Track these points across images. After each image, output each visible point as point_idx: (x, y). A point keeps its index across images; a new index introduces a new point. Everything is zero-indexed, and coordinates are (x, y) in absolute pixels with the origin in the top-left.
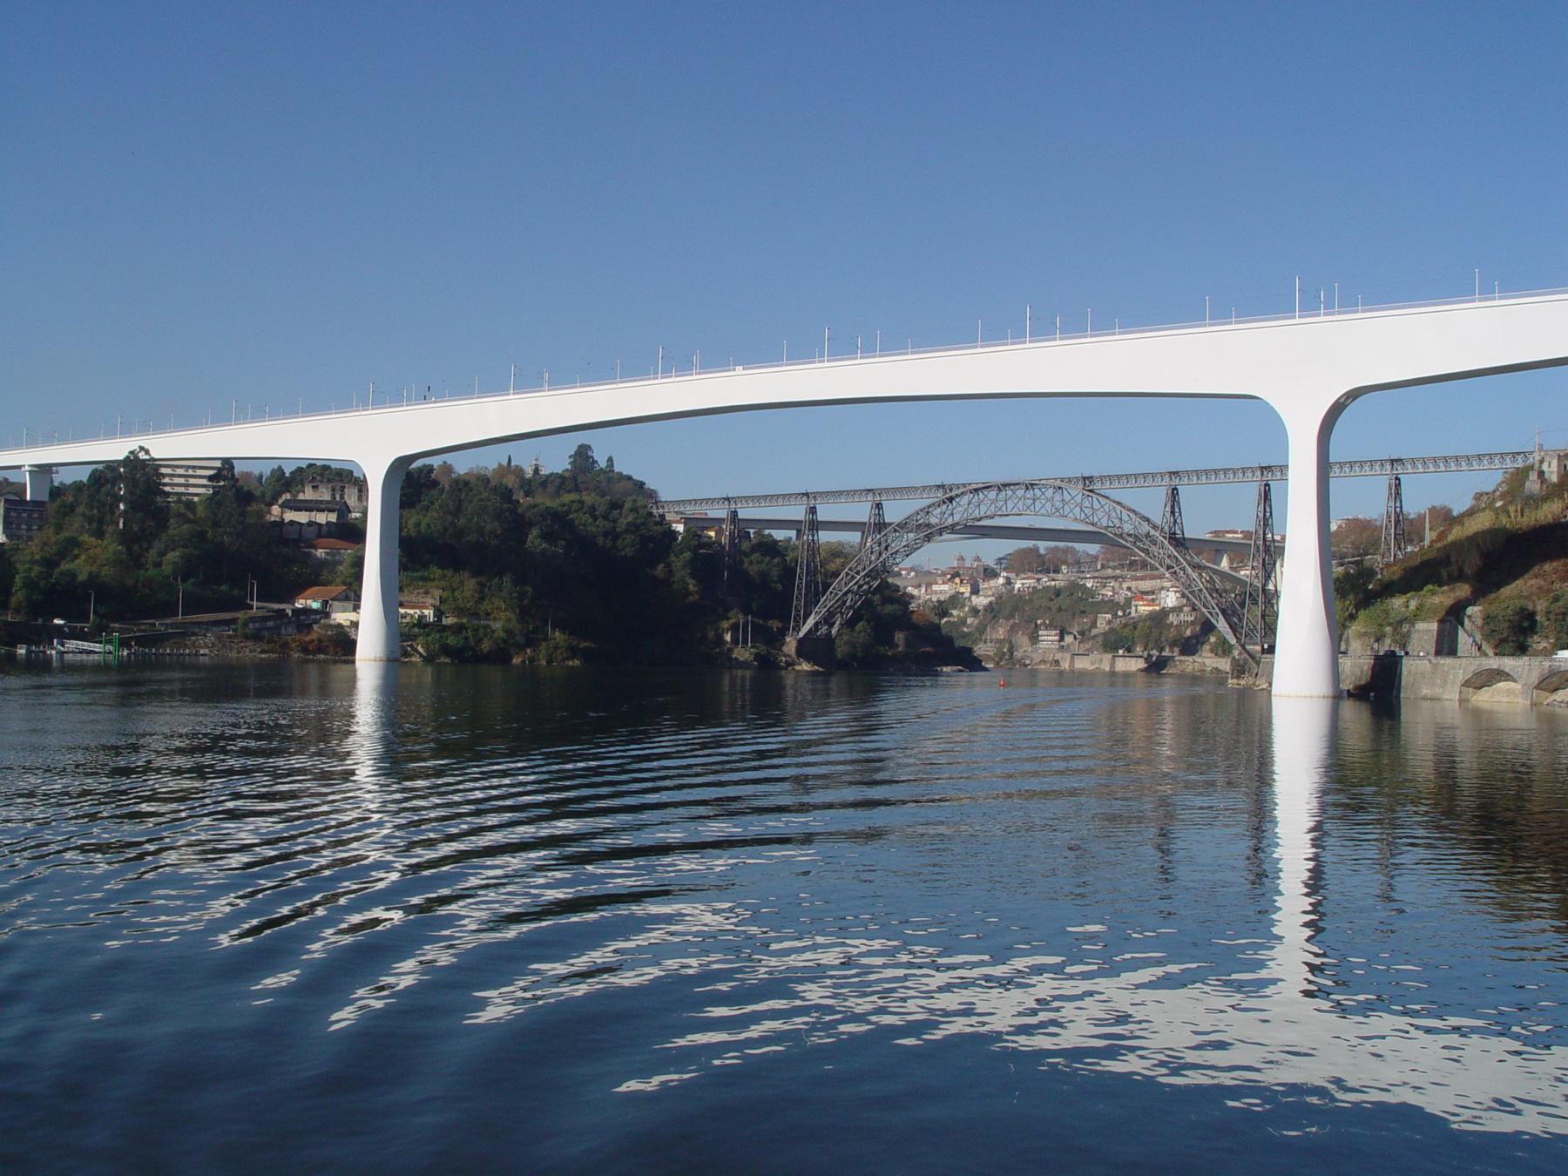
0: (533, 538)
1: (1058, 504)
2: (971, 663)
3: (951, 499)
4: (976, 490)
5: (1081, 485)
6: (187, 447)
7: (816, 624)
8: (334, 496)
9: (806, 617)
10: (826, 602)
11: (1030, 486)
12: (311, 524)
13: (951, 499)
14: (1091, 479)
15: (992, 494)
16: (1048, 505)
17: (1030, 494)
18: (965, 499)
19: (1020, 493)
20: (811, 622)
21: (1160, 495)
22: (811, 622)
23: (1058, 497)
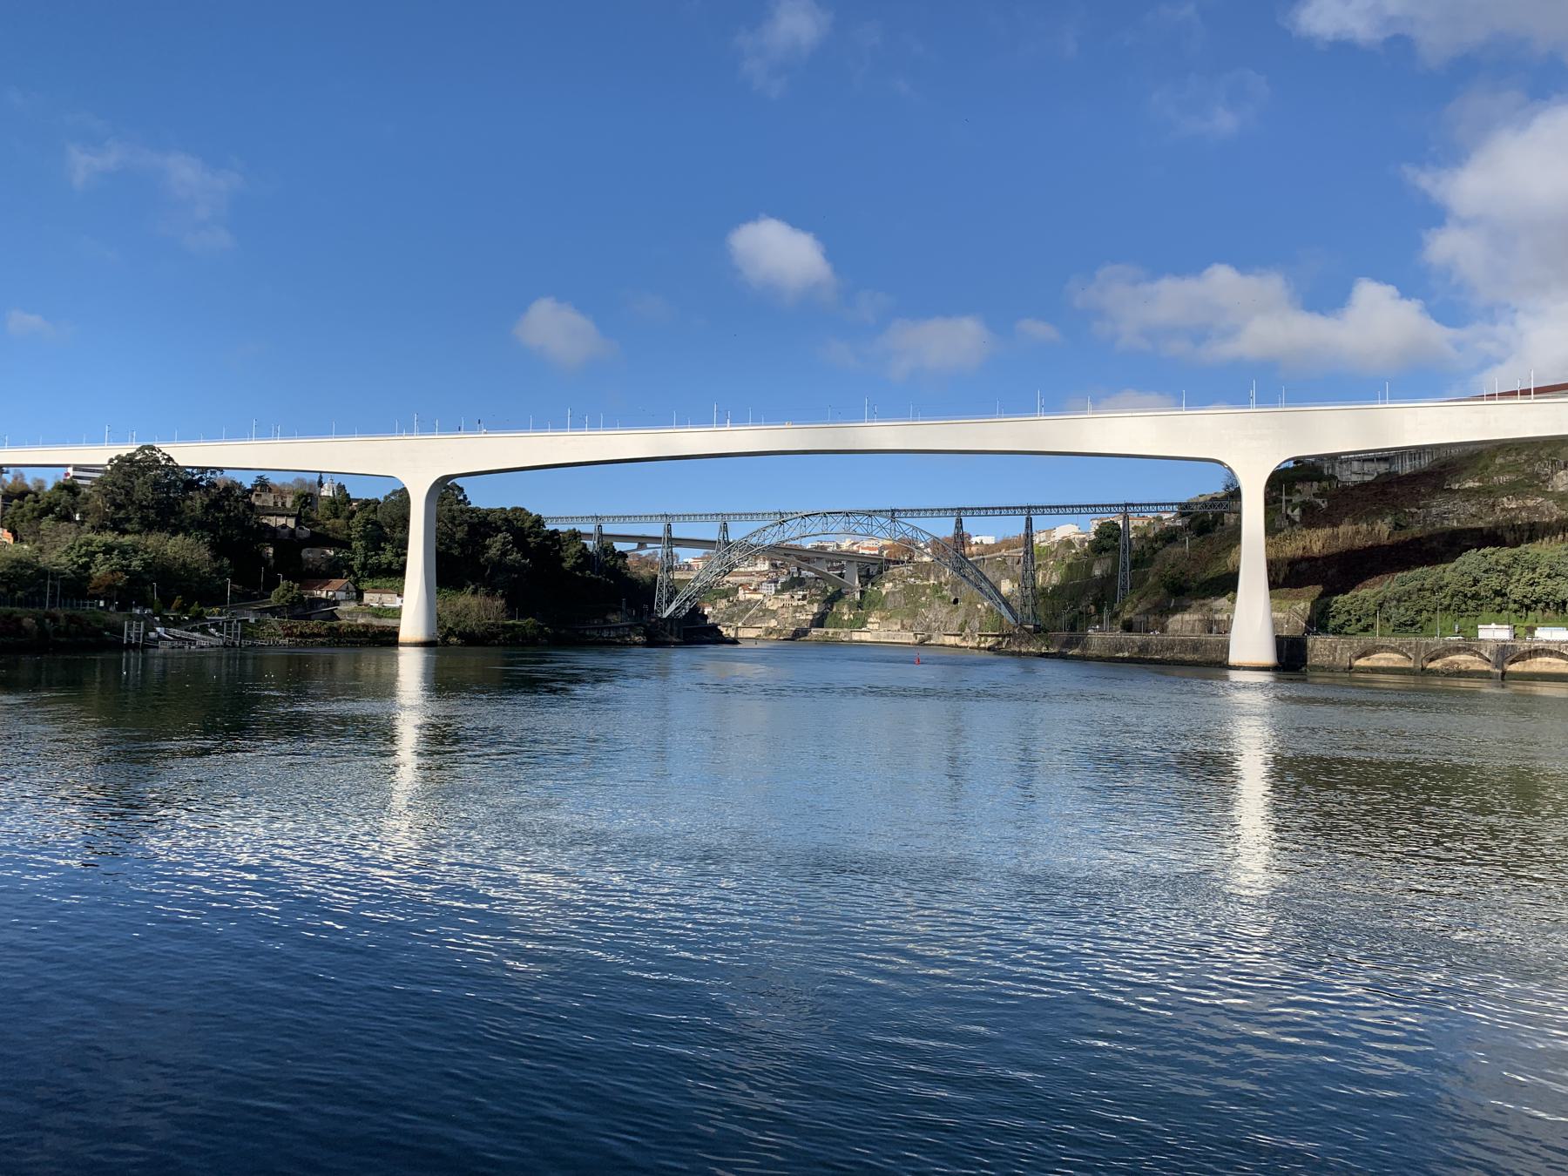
6: (188, 454)
9: (669, 602)
12: (284, 526)
20: (673, 606)
22: (673, 606)
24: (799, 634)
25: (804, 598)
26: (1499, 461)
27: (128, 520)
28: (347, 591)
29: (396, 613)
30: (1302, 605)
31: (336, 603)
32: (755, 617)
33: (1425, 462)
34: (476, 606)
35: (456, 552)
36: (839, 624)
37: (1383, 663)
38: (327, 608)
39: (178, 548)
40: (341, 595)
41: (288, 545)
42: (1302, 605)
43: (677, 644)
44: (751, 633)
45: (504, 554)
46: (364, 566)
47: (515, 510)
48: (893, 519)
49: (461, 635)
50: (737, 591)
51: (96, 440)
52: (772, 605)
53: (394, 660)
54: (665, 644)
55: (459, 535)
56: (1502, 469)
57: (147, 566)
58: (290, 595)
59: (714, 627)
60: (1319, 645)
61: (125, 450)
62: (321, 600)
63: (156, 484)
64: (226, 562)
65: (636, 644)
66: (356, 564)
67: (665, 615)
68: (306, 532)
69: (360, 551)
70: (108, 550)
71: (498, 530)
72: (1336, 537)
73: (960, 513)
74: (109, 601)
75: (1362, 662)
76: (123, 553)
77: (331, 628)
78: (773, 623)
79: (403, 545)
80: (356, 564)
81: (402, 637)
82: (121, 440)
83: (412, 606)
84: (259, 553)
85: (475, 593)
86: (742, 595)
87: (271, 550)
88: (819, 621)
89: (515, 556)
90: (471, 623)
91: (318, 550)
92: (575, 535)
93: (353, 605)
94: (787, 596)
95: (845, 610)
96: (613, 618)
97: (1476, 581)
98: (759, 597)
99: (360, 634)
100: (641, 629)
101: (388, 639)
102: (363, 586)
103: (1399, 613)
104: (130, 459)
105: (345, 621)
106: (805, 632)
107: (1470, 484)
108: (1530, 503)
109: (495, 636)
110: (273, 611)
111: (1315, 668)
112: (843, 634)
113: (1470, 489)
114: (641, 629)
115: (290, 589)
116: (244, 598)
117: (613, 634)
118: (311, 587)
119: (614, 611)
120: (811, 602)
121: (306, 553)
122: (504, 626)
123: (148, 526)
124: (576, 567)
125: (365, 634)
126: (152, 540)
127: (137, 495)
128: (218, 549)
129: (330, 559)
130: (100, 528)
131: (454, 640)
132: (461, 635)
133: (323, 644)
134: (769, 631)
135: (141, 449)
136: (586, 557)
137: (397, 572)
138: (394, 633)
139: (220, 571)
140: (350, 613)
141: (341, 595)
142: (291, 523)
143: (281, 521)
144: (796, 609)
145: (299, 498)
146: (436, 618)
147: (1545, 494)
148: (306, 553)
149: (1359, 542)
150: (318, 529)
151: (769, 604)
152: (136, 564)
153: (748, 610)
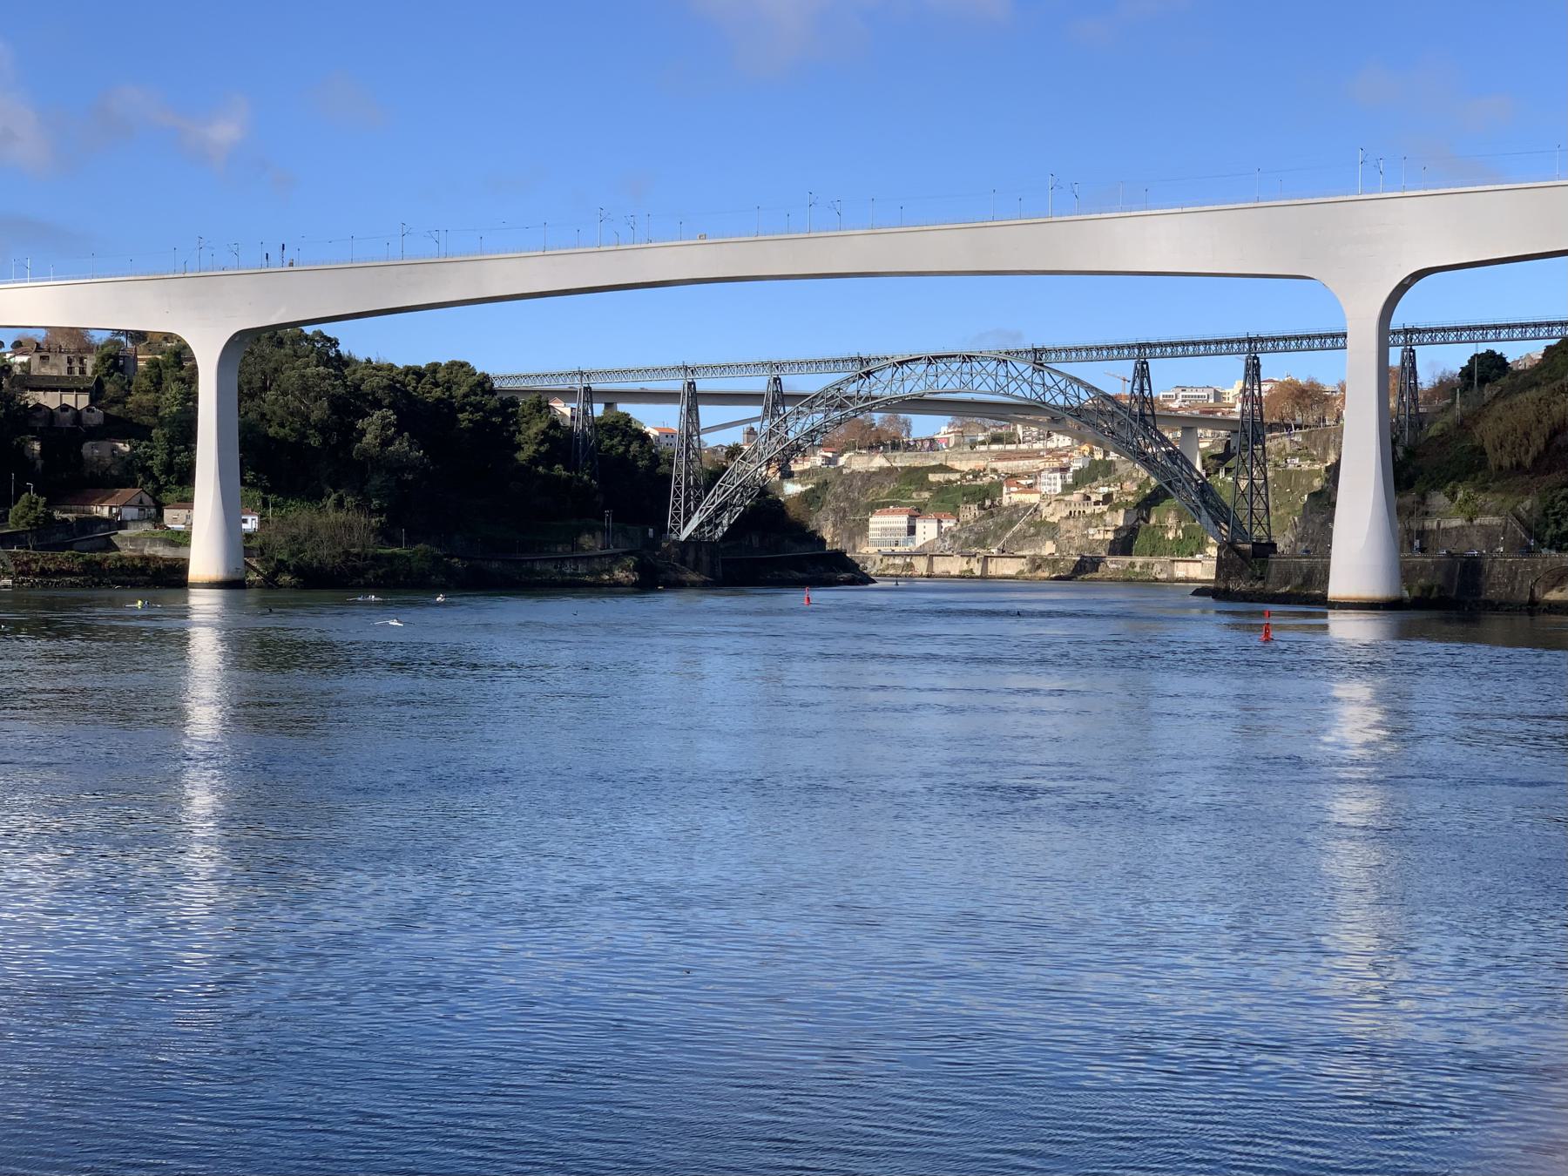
0: (372, 427)
1: (1002, 381)
2: (839, 570)
3: (868, 374)
4: (901, 363)
5: (1030, 357)
7: (701, 525)
8: (70, 370)
9: (688, 516)
10: (714, 499)
13: (868, 374)
14: (1044, 351)
15: (920, 368)
16: (956, 380)
17: (966, 367)
18: (889, 371)
19: (954, 366)
21: (1128, 368)
23: (1002, 371)
24: (1086, 566)
25: (1107, 498)
28: (141, 505)
29: (182, 539)
30: (1528, 503)
31: (123, 525)
32: (1022, 538)
35: (315, 441)
36: (1157, 548)
38: (101, 533)
40: (130, 513)
41: (64, 434)
42: (1528, 503)
44: (1008, 567)
45: (387, 442)
46: (168, 468)
47: (453, 364)
49: (299, 571)
50: (998, 486)
52: (1053, 513)
53: (184, 613)
54: (677, 585)
55: (314, 417)
58: (32, 515)
59: (840, 555)
60: (1497, 568)
62: (101, 520)
65: (618, 584)
66: (155, 464)
67: (684, 536)
68: (97, 417)
69: (163, 443)
71: (377, 404)
73: (1142, 353)
75: (1554, 596)
77: (88, 563)
78: (1049, 548)
83: (205, 532)
84: (21, 448)
85: (340, 504)
86: (1011, 497)
87: (37, 447)
88: (1124, 544)
89: (401, 446)
90: (323, 554)
91: (106, 445)
92: (541, 403)
93: (148, 526)
94: (1076, 496)
95: (1171, 521)
96: (586, 541)
98: (1033, 498)
99: (135, 571)
100: (630, 562)
101: (173, 577)
102: (166, 497)
105: (127, 550)
111: (1495, 607)
114: (630, 562)
115: (32, 506)
117: (582, 568)
118: (89, 501)
119: (591, 531)
120: (1114, 508)
121: (90, 450)
122: (377, 558)
124: (548, 459)
125: (143, 571)
129: (122, 457)
131: (285, 578)
132: (299, 571)
133: (73, 585)
134: (1036, 563)
136: (560, 441)
137: (185, 476)
140: (132, 540)
141: (130, 513)
142: (83, 401)
143: (69, 399)
145: (103, 360)
146: (244, 547)
148: (92, 450)
150: (114, 410)
151: (1046, 511)
153: (1011, 523)
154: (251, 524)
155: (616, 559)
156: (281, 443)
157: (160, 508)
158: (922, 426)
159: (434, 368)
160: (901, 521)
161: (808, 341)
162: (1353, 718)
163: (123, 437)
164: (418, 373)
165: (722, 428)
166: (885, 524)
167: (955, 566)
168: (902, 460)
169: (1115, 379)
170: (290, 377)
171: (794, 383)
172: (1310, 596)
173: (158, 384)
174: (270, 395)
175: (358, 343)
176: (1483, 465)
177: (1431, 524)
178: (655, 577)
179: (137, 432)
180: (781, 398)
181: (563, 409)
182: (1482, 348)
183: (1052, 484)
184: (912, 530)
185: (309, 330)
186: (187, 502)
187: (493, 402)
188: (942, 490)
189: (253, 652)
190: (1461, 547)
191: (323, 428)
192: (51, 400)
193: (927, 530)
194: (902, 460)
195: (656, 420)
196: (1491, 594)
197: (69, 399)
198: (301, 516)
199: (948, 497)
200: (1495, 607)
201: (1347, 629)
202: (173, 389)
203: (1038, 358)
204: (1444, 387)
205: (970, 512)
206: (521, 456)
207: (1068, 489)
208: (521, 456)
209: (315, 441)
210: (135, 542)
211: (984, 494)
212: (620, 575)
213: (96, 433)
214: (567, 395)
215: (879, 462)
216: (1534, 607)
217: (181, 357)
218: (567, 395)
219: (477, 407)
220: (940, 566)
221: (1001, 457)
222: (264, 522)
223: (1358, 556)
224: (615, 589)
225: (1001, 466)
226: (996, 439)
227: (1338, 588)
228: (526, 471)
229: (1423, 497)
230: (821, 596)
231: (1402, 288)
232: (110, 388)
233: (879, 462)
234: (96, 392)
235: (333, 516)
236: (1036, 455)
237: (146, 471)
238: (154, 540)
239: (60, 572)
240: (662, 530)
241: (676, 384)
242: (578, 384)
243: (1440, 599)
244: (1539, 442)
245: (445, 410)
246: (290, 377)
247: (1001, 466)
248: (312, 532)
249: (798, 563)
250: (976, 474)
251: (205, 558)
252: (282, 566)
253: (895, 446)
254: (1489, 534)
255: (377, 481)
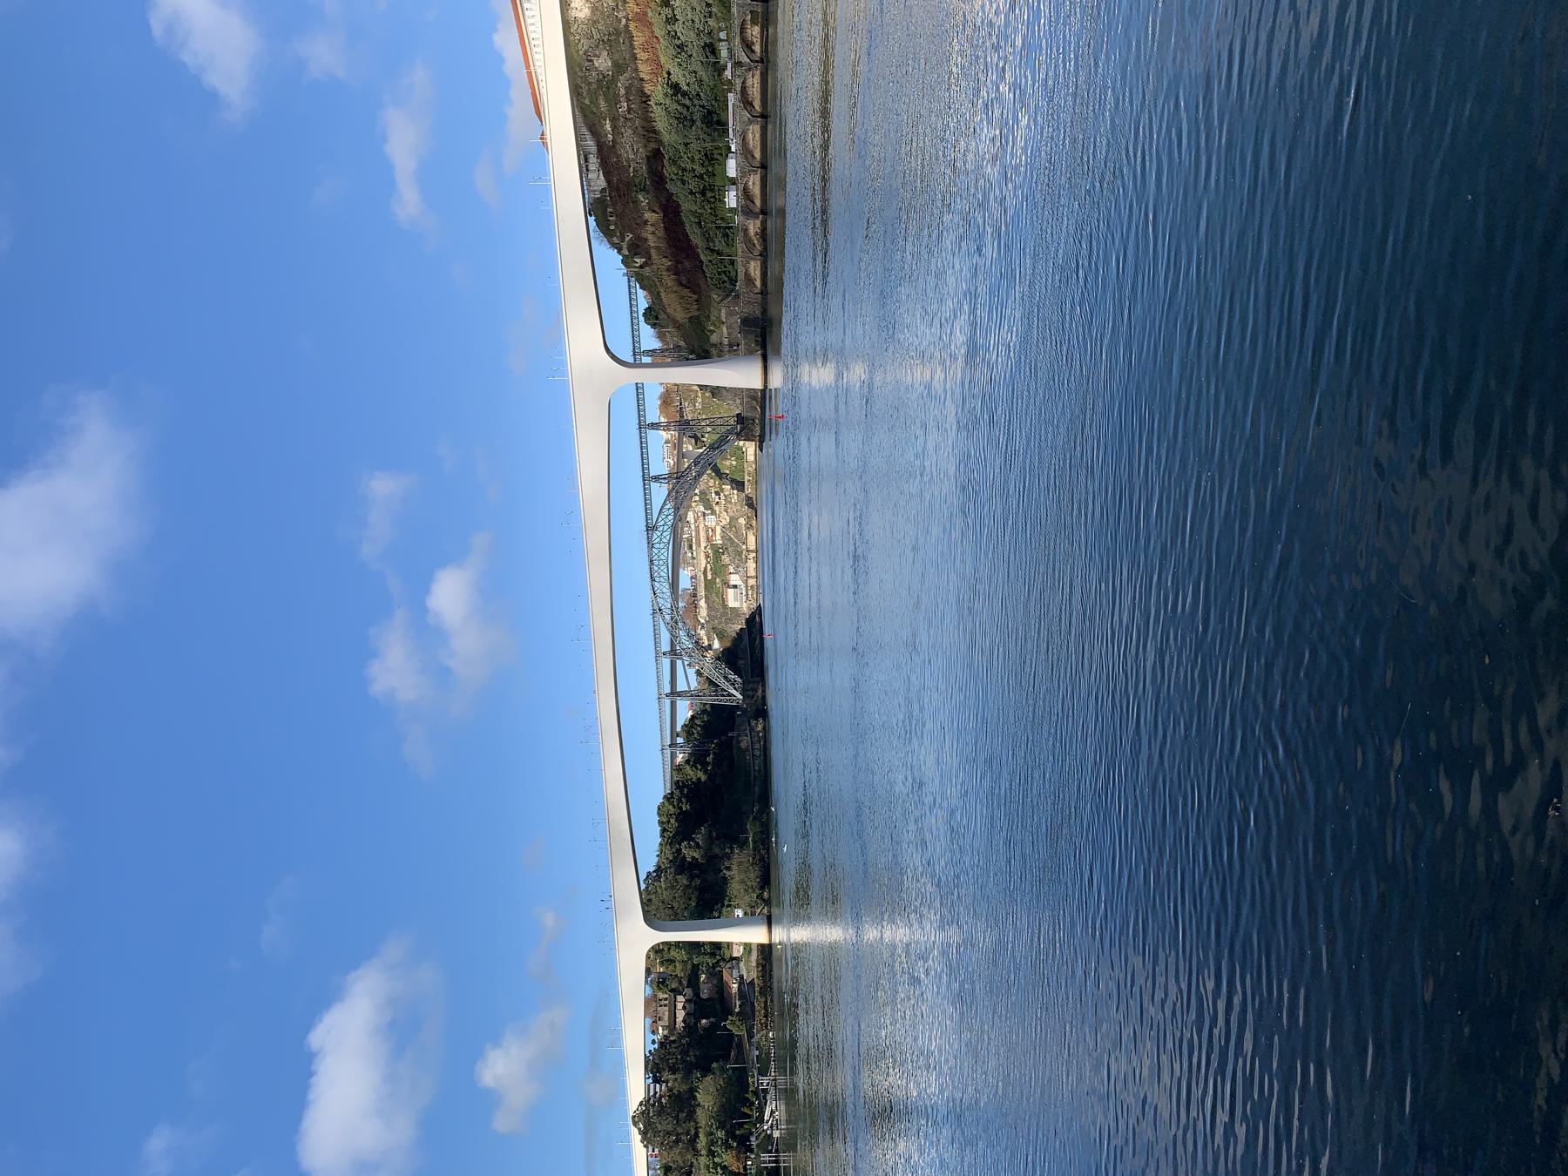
0: (690, 854)
2: (754, 622)
6: (637, 1087)
9: (730, 695)
11: (651, 561)
24: (750, 503)
25: (717, 493)
26: (587, 102)
27: (688, 1133)
31: (741, 977)
33: (584, 130)
34: (739, 873)
35: (698, 881)
37: (758, 273)
38: (746, 988)
39: (707, 1096)
40: (735, 972)
41: (698, 1007)
43: (764, 686)
44: (751, 540)
46: (713, 955)
48: (654, 528)
49: (762, 888)
51: (628, 1150)
55: (685, 882)
56: (595, 102)
57: (721, 1126)
61: (636, 1136)
63: (659, 1114)
64: (715, 1065)
66: (711, 961)
69: (701, 958)
70: (711, 1154)
72: (657, 248)
73: (648, 479)
74: (747, 1158)
75: (758, 283)
76: (712, 1143)
78: (742, 521)
79: (695, 946)
80: (711, 961)
81: (765, 941)
82: (628, 1133)
83: (741, 935)
84: (705, 1029)
85: (728, 868)
86: (718, 540)
88: (739, 485)
89: (699, 839)
90: (753, 875)
92: (678, 769)
94: (717, 508)
96: (743, 745)
97: (691, 193)
98: (718, 530)
100: (753, 723)
101: (766, 951)
102: (727, 957)
103: (719, 244)
104: (644, 1134)
105: (754, 975)
106: (749, 498)
107: (608, 127)
108: (622, 92)
109: (762, 859)
110: (751, 1036)
111: (764, 311)
112: (750, 469)
113: (614, 127)
114: (753, 723)
115: (733, 1023)
116: (741, 1057)
121: (705, 995)
123: (691, 1115)
124: (704, 764)
126: (702, 1117)
127: (670, 1128)
128: (706, 1071)
130: (696, 1153)
132: (762, 888)
135: (635, 1124)
136: (696, 759)
137: (717, 946)
138: (762, 947)
139: (723, 1070)
142: (680, 998)
143: (680, 1006)
144: (728, 501)
146: (750, 918)
147: (614, 80)
148: (705, 995)
149: (661, 233)
152: (720, 1134)
154: (739, 913)
155: (752, 730)
156: (699, 900)
157: (732, 959)
158: (685, 582)
159: (661, 823)
160: (731, 592)
161: (644, 638)
162: (818, 376)
163: (698, 978)
164: (664, 831)
165: (688, 679)
166: (733, 599)
167: (751, 565)
168: (702, 592)
169: (660, 492)
170: (666, 895)
171: (666, 647)
172: (762, 398)
173: (671, 961)
174: (676, 905)
175: (649, 862)
176: (697, 318)
177: (726, 341)
178: (762, 712)
179: (695, 970)
180: (673, 651)
181: (680, 758)
182: (642, 319)
183: (711, 521)
184: (735, 587)
185: (643, 886)
186: (729, 945)
187: (677, 792)
188: (714, 573)
189: (803, 909)
190: (736, 326)
191: (691, 878)
192: (681, 1015)
193: (735, 579)
194: (702, 592)
195: (685, 712)
196: (758, 313)
197: (680, 1006)
198: (735, 887)
199: (719, 569)
200: (764, 311)
201: (776, 380)
202: (674, 953)
203: (651, 528)
204: (661, 336)
205: (726, 559)
206: (703, 778)
207: (713, 512)
208: (703, 778)
209: (698, 881)
210: (749, 970)
211: (717, 553)
212: (760, 727)
213: (697, 993)
214: (673, 756)
215: (702, 603)
216: (764, 293)
217: (658, 950)
218: (673, 756)
219: (680, 801)
220: (752, 573)
221: (699, 545)
222: (738, 906)
223: (741, 375)
224: (766, 730)
225: (703, 544)
226: (690, 547)
227: (758, 385)
228: (711, 776)
229: (714, 345)
230: (767, 630)
231: (614, 357)
232: (674, 986)
233: (702, 603)
234: (676, 992)
235: (734, 872)
236: (697, 528)
237: (714, 966)
238: (748, 961)
239: (766, 1008)
240: (737, 707)
241: (667, 702)
242: (668, 752)
243: (762, 336)
244: (686, 292)
245: (682, 817)
246: (666, 895)
247: (703, 544)
248: (743, 882)
249: (752, 642)
250: (707, 557)
251: (756, 935)
252: (760, 896)
253: (695, 596)
254: (730, 314)
255: (717, 850)
